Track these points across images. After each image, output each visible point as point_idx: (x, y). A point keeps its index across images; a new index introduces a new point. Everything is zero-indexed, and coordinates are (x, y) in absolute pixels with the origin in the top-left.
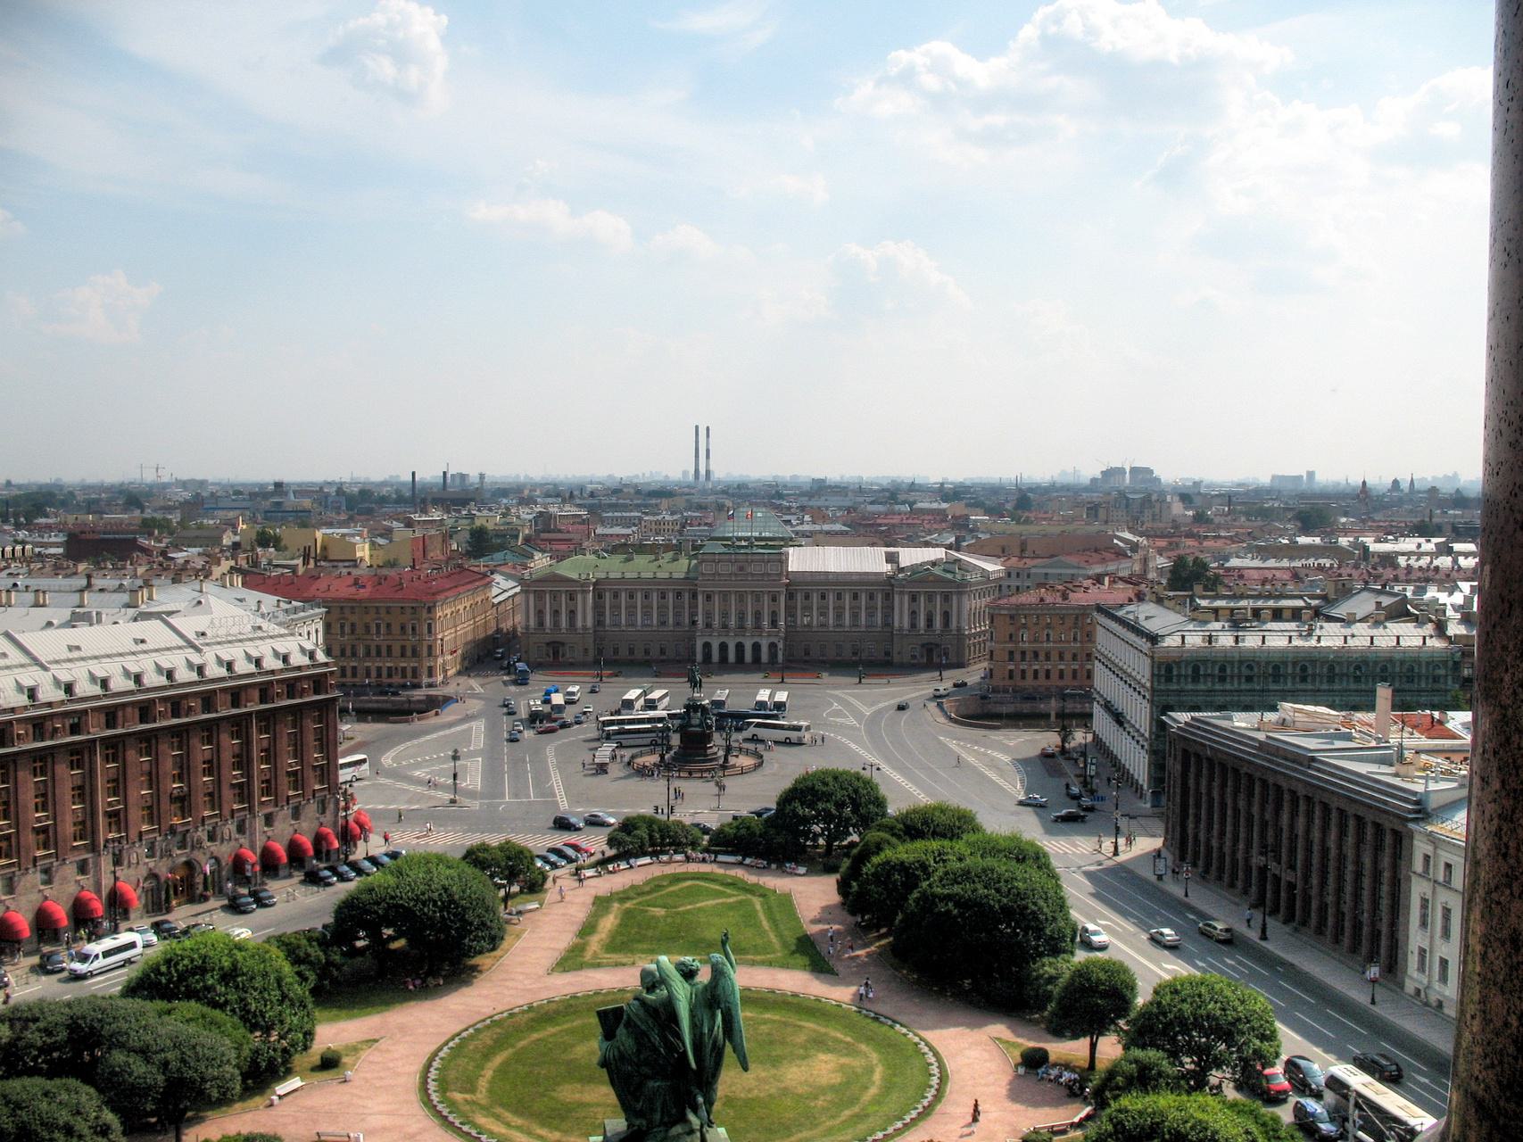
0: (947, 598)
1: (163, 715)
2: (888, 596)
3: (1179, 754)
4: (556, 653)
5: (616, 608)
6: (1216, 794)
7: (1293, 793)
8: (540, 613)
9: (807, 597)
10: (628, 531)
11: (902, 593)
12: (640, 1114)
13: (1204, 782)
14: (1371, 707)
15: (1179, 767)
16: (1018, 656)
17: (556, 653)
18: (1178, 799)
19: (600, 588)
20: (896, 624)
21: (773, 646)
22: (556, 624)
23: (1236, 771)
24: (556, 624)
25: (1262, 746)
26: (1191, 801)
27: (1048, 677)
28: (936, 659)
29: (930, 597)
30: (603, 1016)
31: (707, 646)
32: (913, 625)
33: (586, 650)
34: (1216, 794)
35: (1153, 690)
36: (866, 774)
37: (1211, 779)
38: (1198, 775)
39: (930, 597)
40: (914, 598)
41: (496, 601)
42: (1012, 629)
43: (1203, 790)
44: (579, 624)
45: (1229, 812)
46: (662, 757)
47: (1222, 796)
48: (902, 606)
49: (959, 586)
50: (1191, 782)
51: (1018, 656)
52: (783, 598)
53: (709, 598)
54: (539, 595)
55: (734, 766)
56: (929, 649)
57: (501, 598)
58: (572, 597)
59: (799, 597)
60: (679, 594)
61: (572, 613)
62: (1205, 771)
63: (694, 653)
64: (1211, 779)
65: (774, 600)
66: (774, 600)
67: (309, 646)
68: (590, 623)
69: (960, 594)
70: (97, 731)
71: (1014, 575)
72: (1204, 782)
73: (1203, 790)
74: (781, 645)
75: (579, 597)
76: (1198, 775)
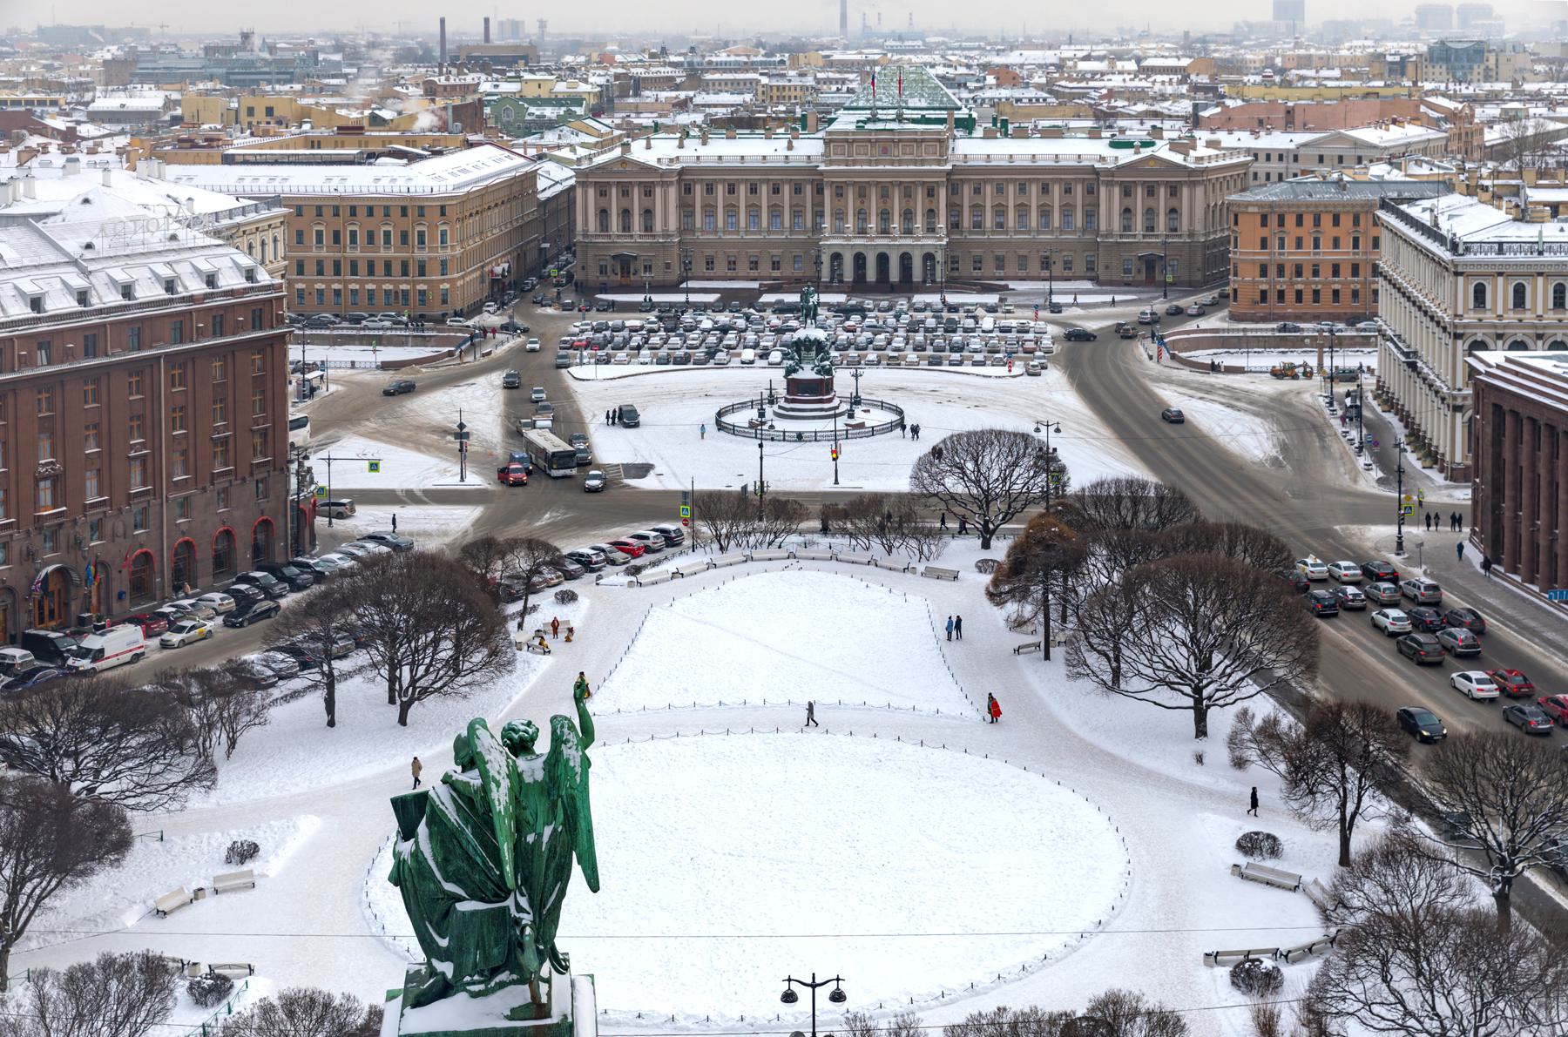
0: (1174, 190)
2: (1091, 191)
3: (1490, 409)
4: (626, 270)
5: (710, 210)
6: (1542, 471)
8: (603, 213)
9: (977, 191)
10: (737, 99)
11: (1109, 184)
12: (444, 955)
13: (1525, 449)
15: (1489, 430)
16: (1273, 271)
17: (626, 270)
18: (1489, 476)
19: (686, 179)
20: (1103, 227)
21: (929, 257)
22: (626, 227)
24: (626, 227)
26: (1508, 478)
27: (1316, 300)
28: (1159, 277)
29: (1151, 191)
30: (395, 802)
31: (837, 257)
32: (1127, 228)
33: (668, 266)
34: (1542, 471)
36: (1042, 436)
37: (1536, 447)
38: (1517, 441)
39: (1151, 191)
40: (1127, 191)
41: (542, 196)
42: (1264, 232)
43: (1524, 462)
44: (658, 227)
46: (762, 415)
47: (1552, 471)
48: (1110, 202)
49: (1192, 172)
50: (1507, 454)
51: (1273, 271)
52: (943, 193)
53: (839, 192)
54: (603, 192)
55: (862, 425)
56: (1150, 263)
57: (548, 194)
58: (648, 192)
59: (967, 191)
60: (798, 190)
61: (648, 213)
62: (1526, 437)
63: (819, 271)
64: (1536, 447)
66: (931, 192)
68: (673, 225)
69: (1193, 184)
71: (1274, 157)
72: (1525, 449)
73: (1524, 462)
74: (939, 257)
75: (658, 191)
76: (1517, 441)
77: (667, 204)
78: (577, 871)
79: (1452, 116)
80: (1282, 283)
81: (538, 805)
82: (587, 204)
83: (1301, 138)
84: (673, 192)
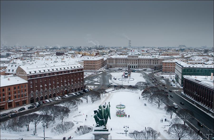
1: (63, 73)
7: (199, 86)
14: (211, 76)
23: (192, 83)
25: (195, 80)
26: (186, 86)
35: (182, 73)
40: (153, 61)
45: (191, 88)
48: (152, 61)
50: (186, 84)
54: (109, 60)
57: (105, 60)
65: (137, 61)
66: (137, 61)
67: (81, 65)
70: (56, 75)
73: (188, 85)
74: (137, 66)
76: (187, 83)
77: (114, 61)
78: (109, 117)
79: (182, 55)
80: (167, 69)
81: (106, 112)
82: (108, 61)
83: (168, 56)
84: (115, 60)
